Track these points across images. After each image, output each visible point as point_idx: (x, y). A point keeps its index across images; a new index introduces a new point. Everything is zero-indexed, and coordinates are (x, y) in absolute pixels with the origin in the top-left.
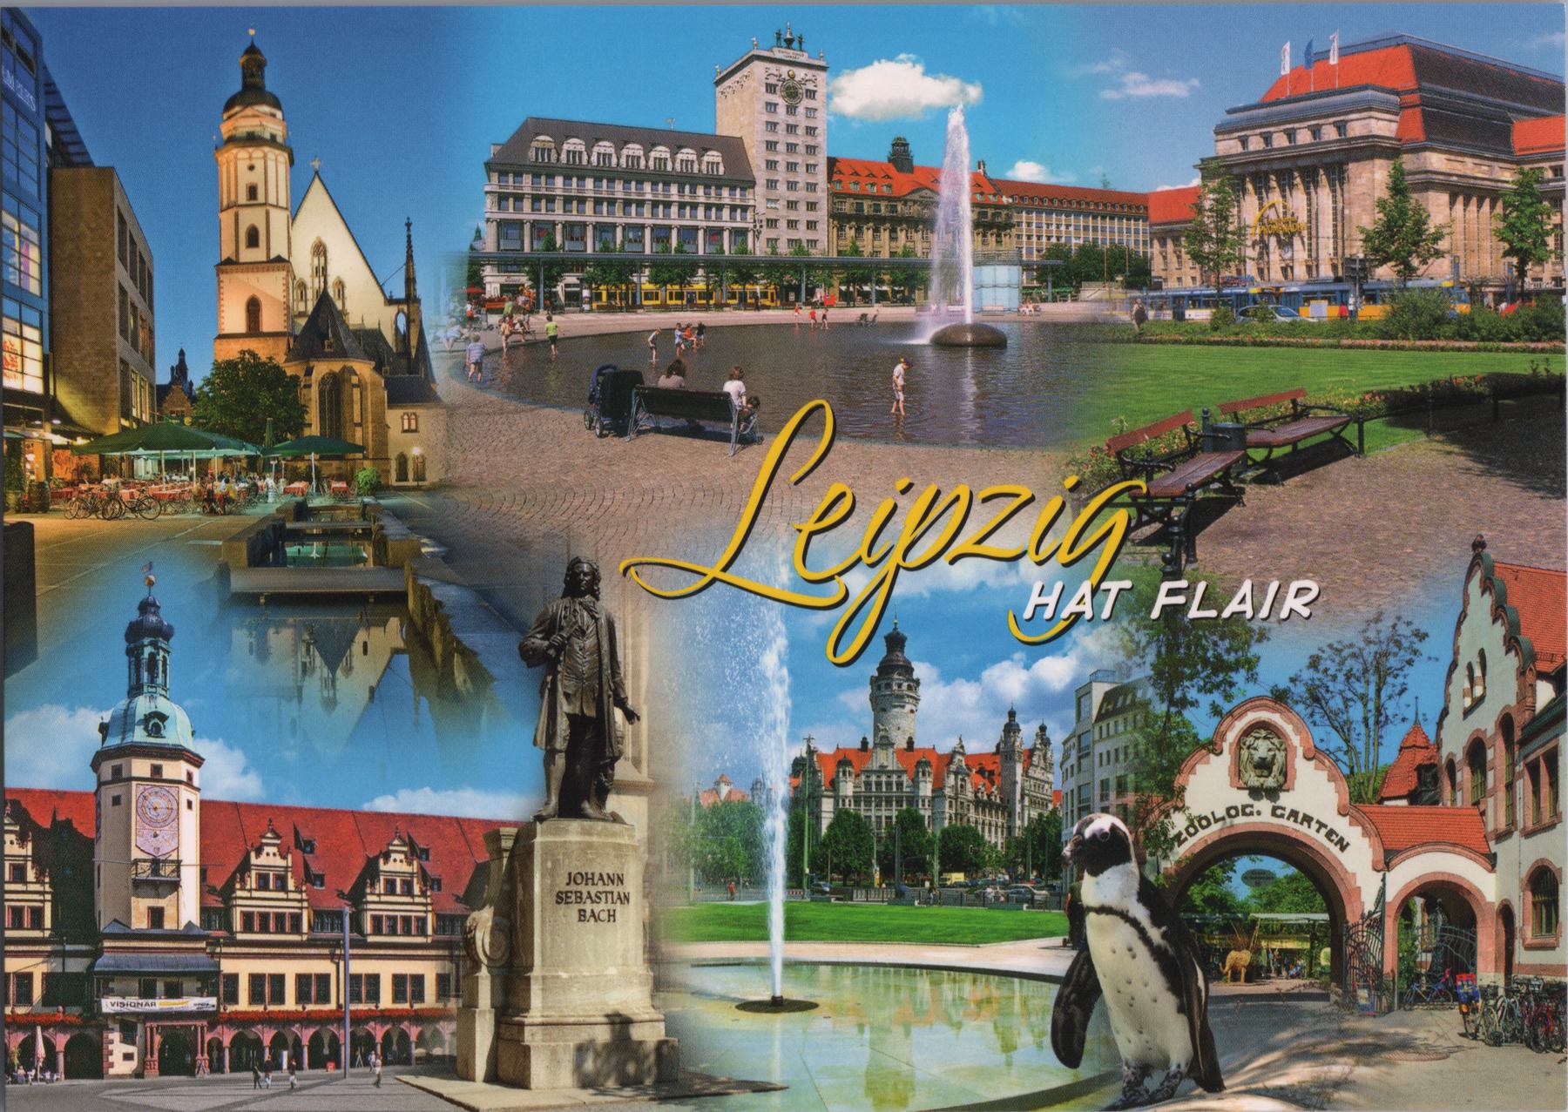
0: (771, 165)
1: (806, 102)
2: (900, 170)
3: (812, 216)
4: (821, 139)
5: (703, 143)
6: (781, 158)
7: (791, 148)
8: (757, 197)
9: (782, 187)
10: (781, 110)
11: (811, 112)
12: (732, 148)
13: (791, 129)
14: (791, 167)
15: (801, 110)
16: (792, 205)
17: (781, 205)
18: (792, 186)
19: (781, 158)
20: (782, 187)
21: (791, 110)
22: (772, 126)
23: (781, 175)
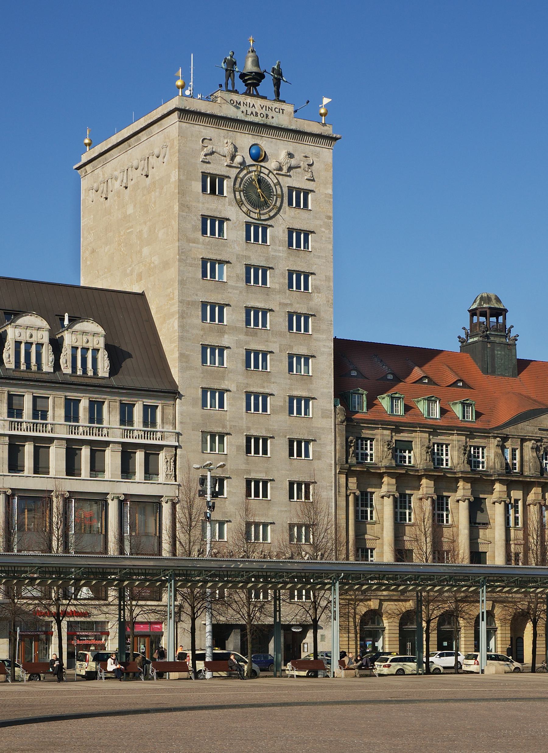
0: (211, 352)
1: (289, 217)
2: (489, 369)
3: (299, 470)
4: (320, 298)
5: (65, 302)
6: (234, 339)
7: (255, 316)
8: (180, 420)
9: (234, 405)
10: (234, 233)
11: (298, 238)
12: (123, 315)
13: (255, 274)
14: (254, 359)
15: (277, 232)
16: (255, 444)
17: (233, 445)
18: (256, 401)
19: (234, 339)
20: (234, 405)
21: (255, 232)
22: (209, 267)
23: (234, 376)
